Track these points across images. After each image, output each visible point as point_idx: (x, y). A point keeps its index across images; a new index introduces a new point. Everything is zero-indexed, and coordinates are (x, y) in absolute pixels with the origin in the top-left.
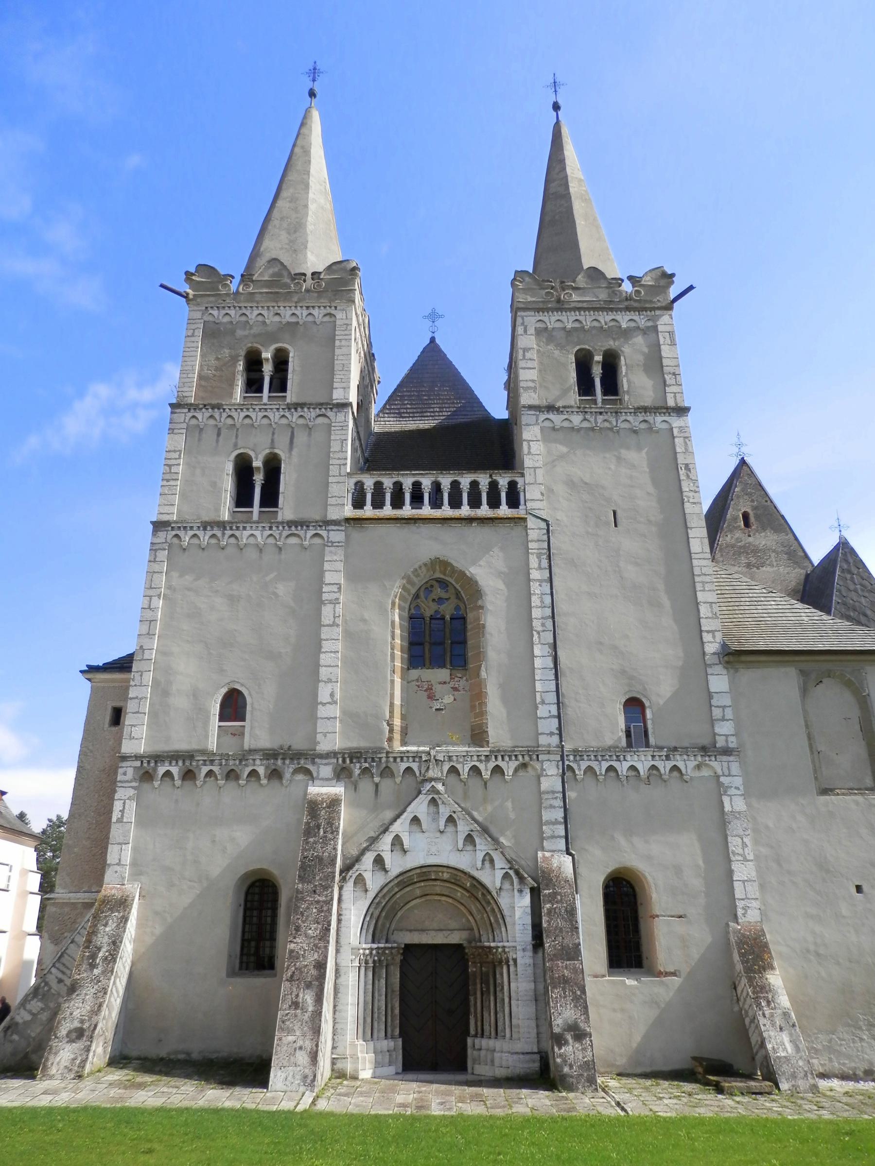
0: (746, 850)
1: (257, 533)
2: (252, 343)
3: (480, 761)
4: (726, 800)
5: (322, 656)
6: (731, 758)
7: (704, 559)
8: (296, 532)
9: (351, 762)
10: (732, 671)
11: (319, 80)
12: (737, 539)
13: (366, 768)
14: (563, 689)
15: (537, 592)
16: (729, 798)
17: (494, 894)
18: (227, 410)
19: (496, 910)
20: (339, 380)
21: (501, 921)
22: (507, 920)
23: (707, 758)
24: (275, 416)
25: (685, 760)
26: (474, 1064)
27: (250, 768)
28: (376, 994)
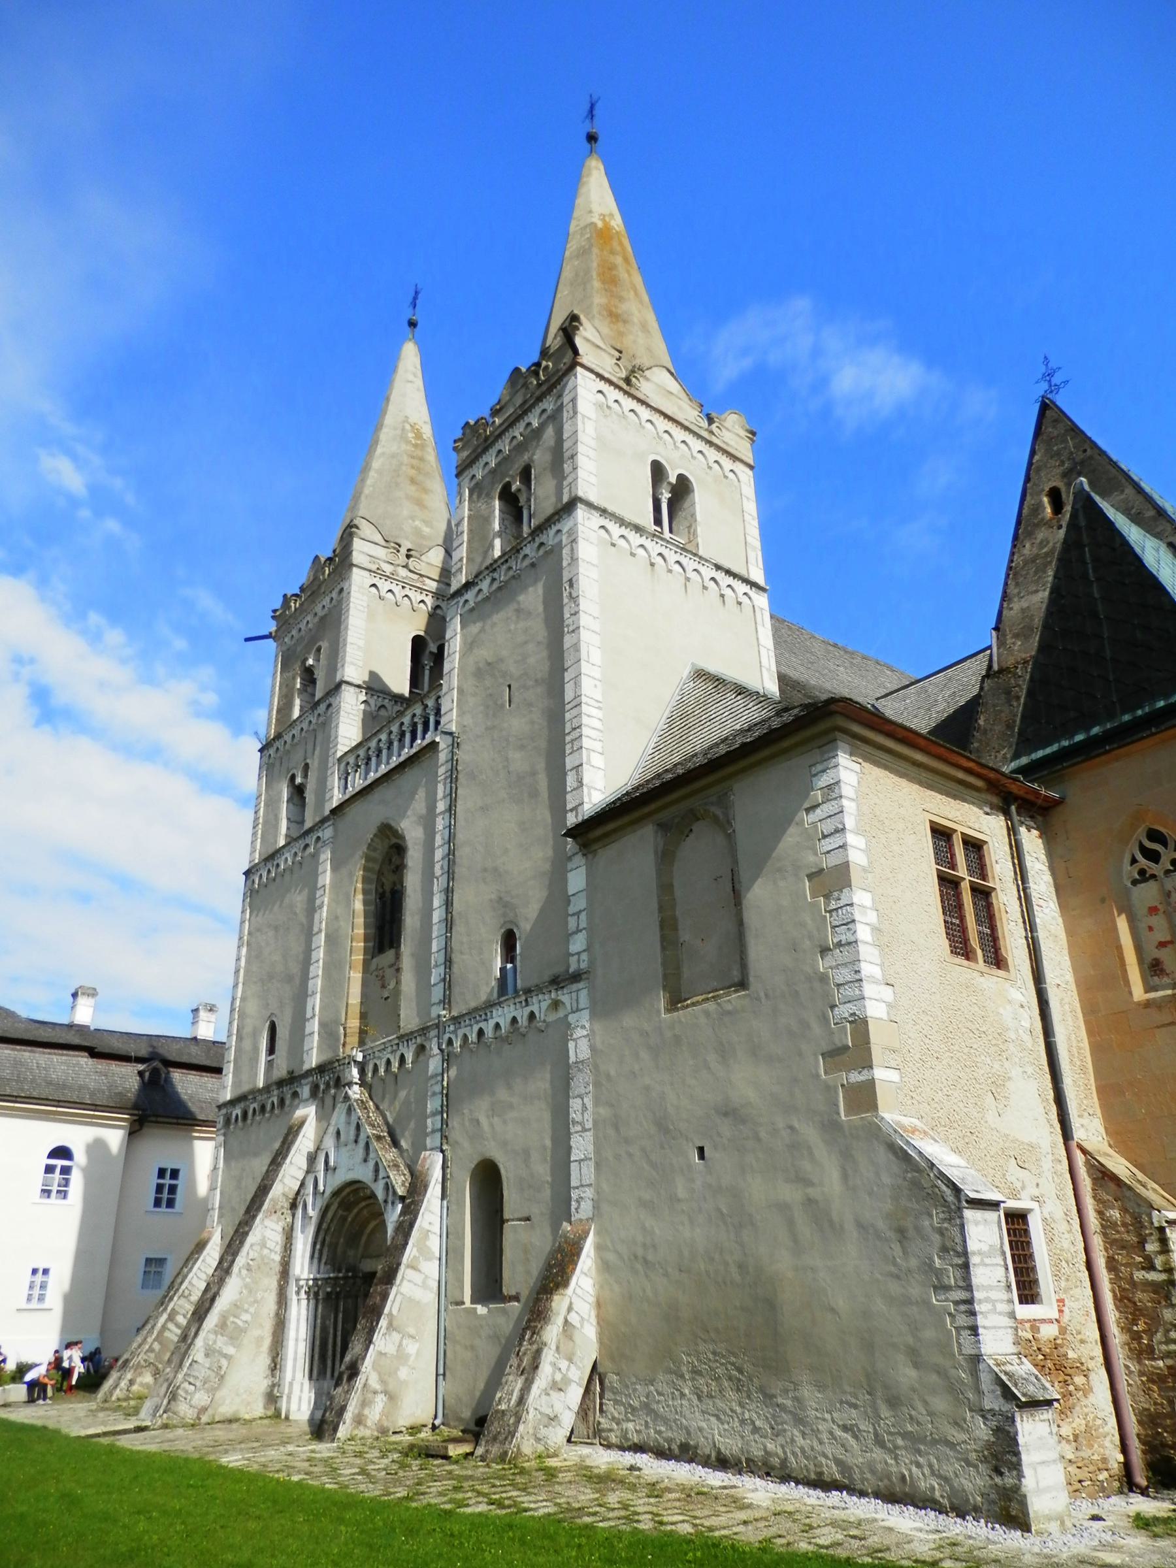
0: (585, 1115)
6: (581, 985)
12: (1041, 542)
14: (455, 944)
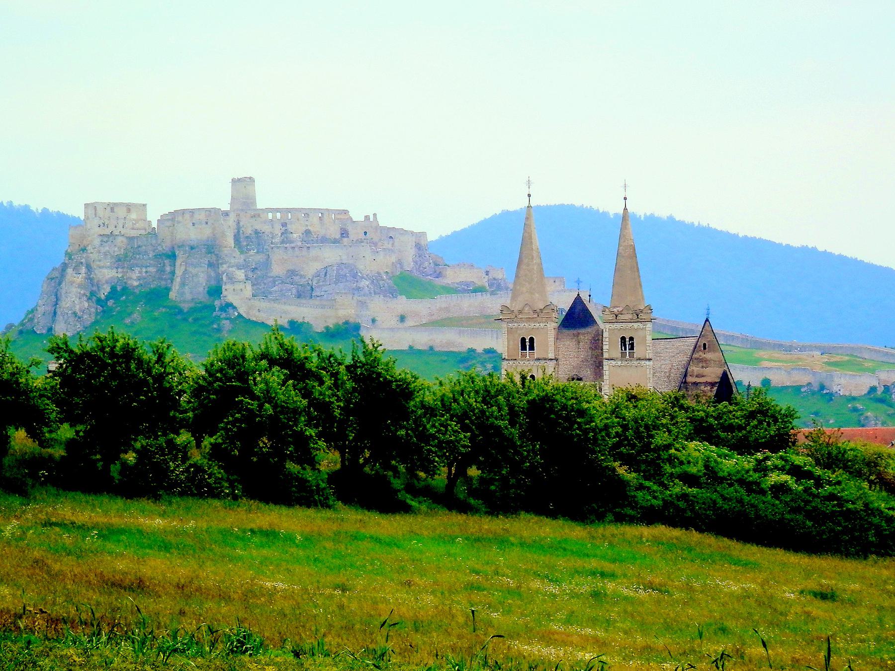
24: (532, 363)
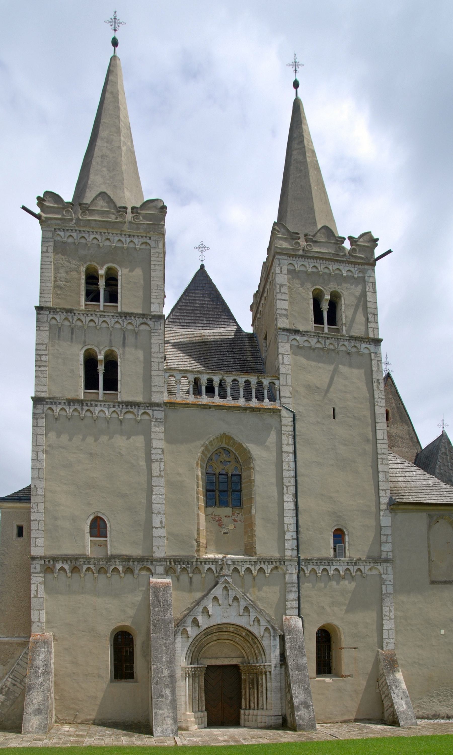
0: (391, 613)
1: (105, 409)
2: (91, 261)
3: (252, 565)
4: (384, 587)
5: (154, 497)
6: (389, 564)
7: (384, 444)
8: (131, 410)
9: (175, 564)
10: (393, 514)
11: (121, 29)
13: (184, 568)
14: (300, 523)
15: (286, 460)
16: (385, 586)
17: (259, 639)
18: (77, 314)
19: (260, 647)
20: (155, 297)
21: (262, 653)
22: (267, 652)
23: (376, 564)
24: (111, 321)
25: (364, 566)
26: (245, 722)
27: (113, 567)
28: (194, 690)
